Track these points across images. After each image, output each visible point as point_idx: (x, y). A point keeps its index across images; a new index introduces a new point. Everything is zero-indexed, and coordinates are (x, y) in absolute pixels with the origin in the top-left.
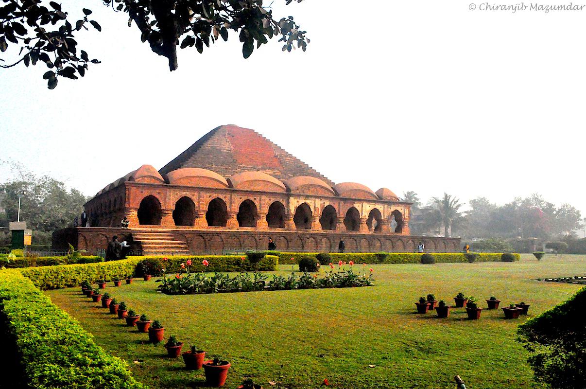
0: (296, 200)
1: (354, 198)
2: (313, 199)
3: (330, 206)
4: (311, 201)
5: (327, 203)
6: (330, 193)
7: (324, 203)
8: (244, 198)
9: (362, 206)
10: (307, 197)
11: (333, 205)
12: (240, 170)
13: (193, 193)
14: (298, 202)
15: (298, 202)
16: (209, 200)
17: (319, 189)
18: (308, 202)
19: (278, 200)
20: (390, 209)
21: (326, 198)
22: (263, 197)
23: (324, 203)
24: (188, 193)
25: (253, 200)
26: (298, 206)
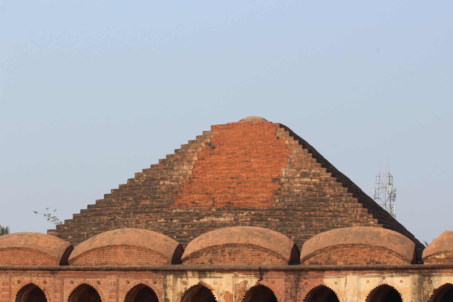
1: (340, 264)
4: (213, 280)
5: (252, 282)
6: (275, 259)
7: (246, 282)
8: (78, 282)
9: (346, 283)
10: (202, 272)
11: (263, 283)
12: (163, 220)
14: (185, 283)
15: (185, 283)
16: (16, 288)
17: (246, 251)
18: (208, 281)
19: (142, 283)
20: (430, 282)
21: (247, 271)
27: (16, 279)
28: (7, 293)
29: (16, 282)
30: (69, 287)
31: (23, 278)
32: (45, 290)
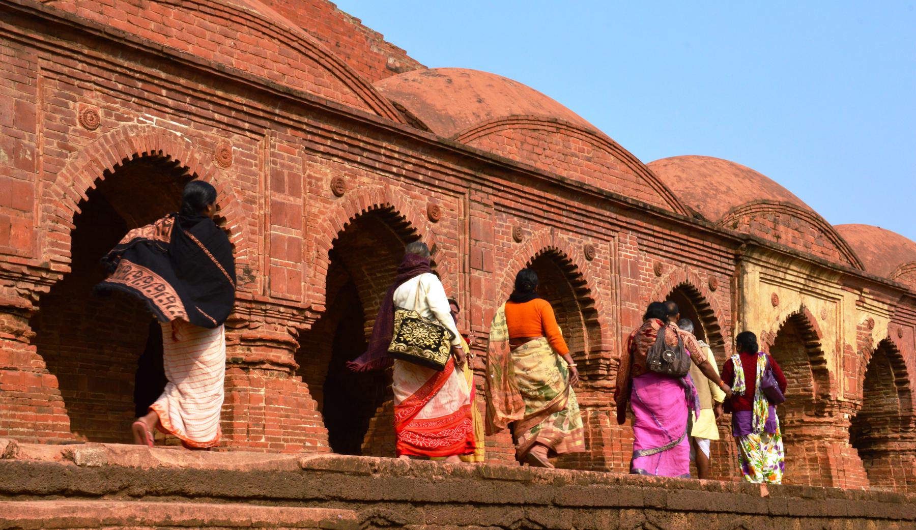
0: (769, 290)
2: (834, 289)
3: (885, 345)
7: (870, 324)
13: (213, 134)
14: (775, 302)
15: (775, 302)
16: (331, 217)
17: (811, 234)
18: (815, 307)
19: (692, 281)
22: (627, 247)
23: (870, 324)
24: (178, 127)
25: (576, 258)
26: (776, 328)
27: (325, 171)
28: (295, 234)
29: (326, 188)
30: (509, 256)
31: (354, 175)
32: (434, 249)
